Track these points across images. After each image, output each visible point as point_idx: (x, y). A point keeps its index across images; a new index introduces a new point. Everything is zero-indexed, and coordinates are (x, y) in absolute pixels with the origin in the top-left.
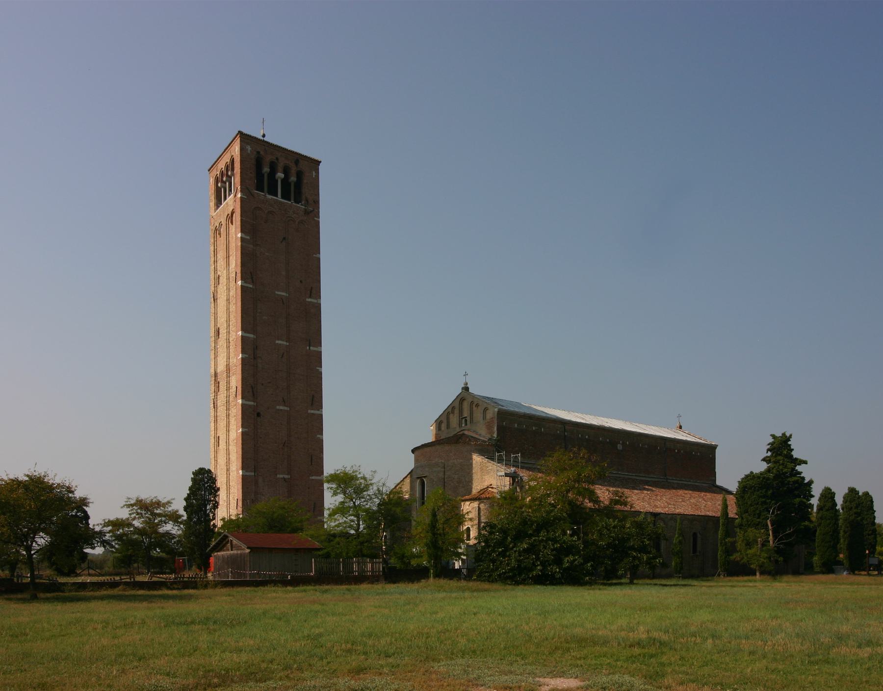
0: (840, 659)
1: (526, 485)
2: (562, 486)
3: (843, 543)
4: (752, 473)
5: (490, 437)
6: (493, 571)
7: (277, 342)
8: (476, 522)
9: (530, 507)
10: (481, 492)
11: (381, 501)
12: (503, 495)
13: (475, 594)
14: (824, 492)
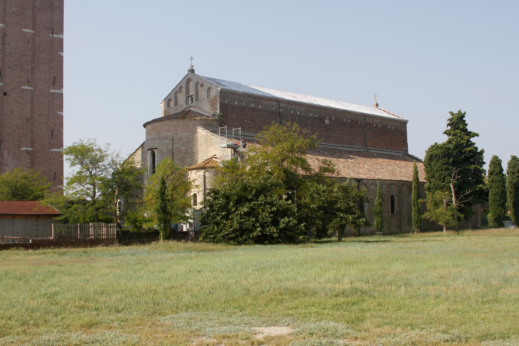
0: (506, 298)
1: (246, 155)
2: (277, 156)
3: (509, 203)
4: (436, 144)
5: (214, 113)
6: (217, 232)
7: (24, 30)
8: (202, 188)
9: (250, 175)
10: (206, 162)
11: (115, 171)
12: (226, 164)
13: (201, 254)
14: (493, 160)
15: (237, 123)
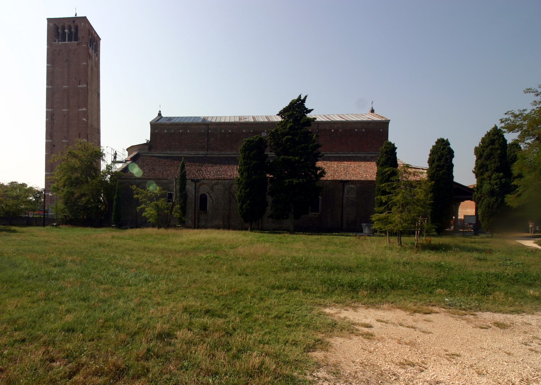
7: (63, 110)
15: (165, 145)
